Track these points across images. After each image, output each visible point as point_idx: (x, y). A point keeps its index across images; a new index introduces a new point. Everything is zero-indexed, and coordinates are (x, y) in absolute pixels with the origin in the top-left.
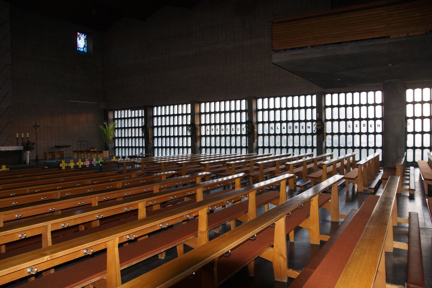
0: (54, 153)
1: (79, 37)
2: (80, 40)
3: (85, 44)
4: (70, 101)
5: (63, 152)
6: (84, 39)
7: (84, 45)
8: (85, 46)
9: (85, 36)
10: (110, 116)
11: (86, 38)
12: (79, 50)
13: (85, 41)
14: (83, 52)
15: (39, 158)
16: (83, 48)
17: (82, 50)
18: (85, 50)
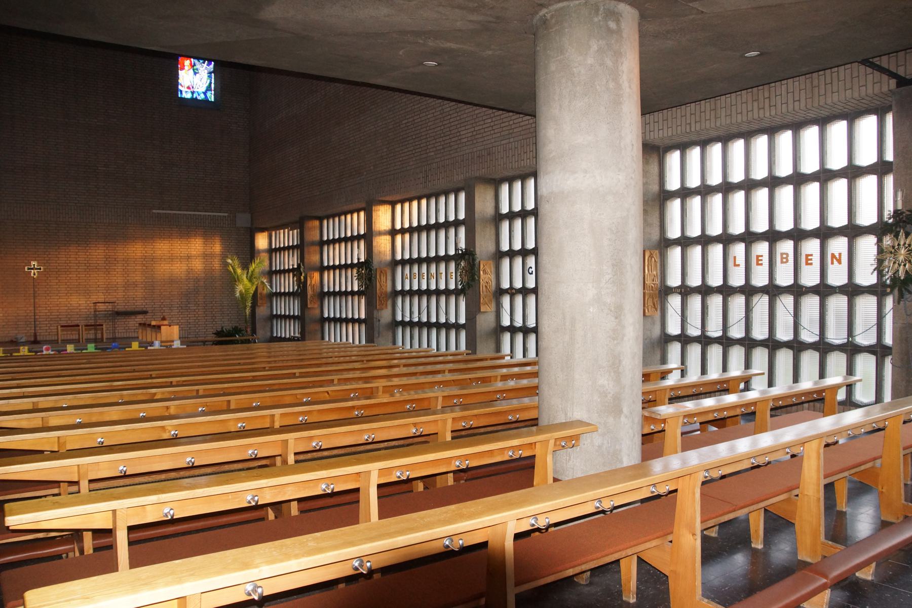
0: (102, 327)
1: (195, 67)
2: (197, 75)
3: (211, 83)
4: (154, 211)
5: (102, 325)
6: (206, 71)
7: (207, 84)
8: (209, 88)
9: (212, 66)
10: (262, 241)
11: (212, 70)
12: (194, 97)
13: (210, 77)
14: (206, 101)
16: (205, 93)
17: (202, 97)
18: (211, 97)
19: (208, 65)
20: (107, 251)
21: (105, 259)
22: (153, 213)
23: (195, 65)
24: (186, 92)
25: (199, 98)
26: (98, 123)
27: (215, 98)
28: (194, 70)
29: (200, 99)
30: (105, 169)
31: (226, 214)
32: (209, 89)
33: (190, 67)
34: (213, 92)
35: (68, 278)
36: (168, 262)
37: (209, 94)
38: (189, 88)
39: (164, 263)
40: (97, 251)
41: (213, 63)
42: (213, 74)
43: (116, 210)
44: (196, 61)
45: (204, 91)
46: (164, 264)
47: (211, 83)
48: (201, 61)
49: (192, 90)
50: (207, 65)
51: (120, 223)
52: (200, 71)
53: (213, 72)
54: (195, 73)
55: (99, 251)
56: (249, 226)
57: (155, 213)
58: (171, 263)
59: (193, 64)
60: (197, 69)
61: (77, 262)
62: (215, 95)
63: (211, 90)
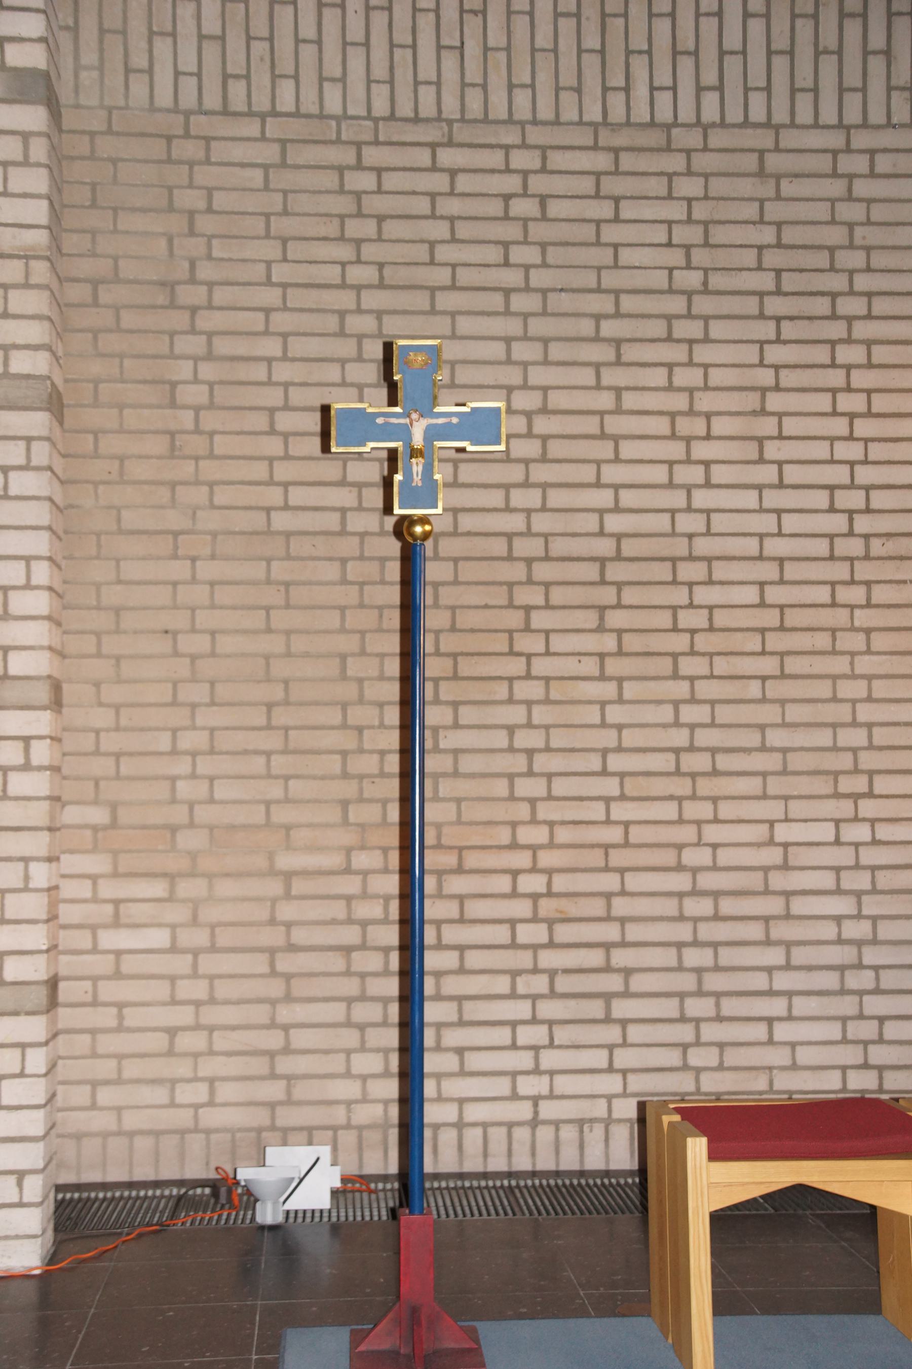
35: (689, 619)
61: (768, 474)
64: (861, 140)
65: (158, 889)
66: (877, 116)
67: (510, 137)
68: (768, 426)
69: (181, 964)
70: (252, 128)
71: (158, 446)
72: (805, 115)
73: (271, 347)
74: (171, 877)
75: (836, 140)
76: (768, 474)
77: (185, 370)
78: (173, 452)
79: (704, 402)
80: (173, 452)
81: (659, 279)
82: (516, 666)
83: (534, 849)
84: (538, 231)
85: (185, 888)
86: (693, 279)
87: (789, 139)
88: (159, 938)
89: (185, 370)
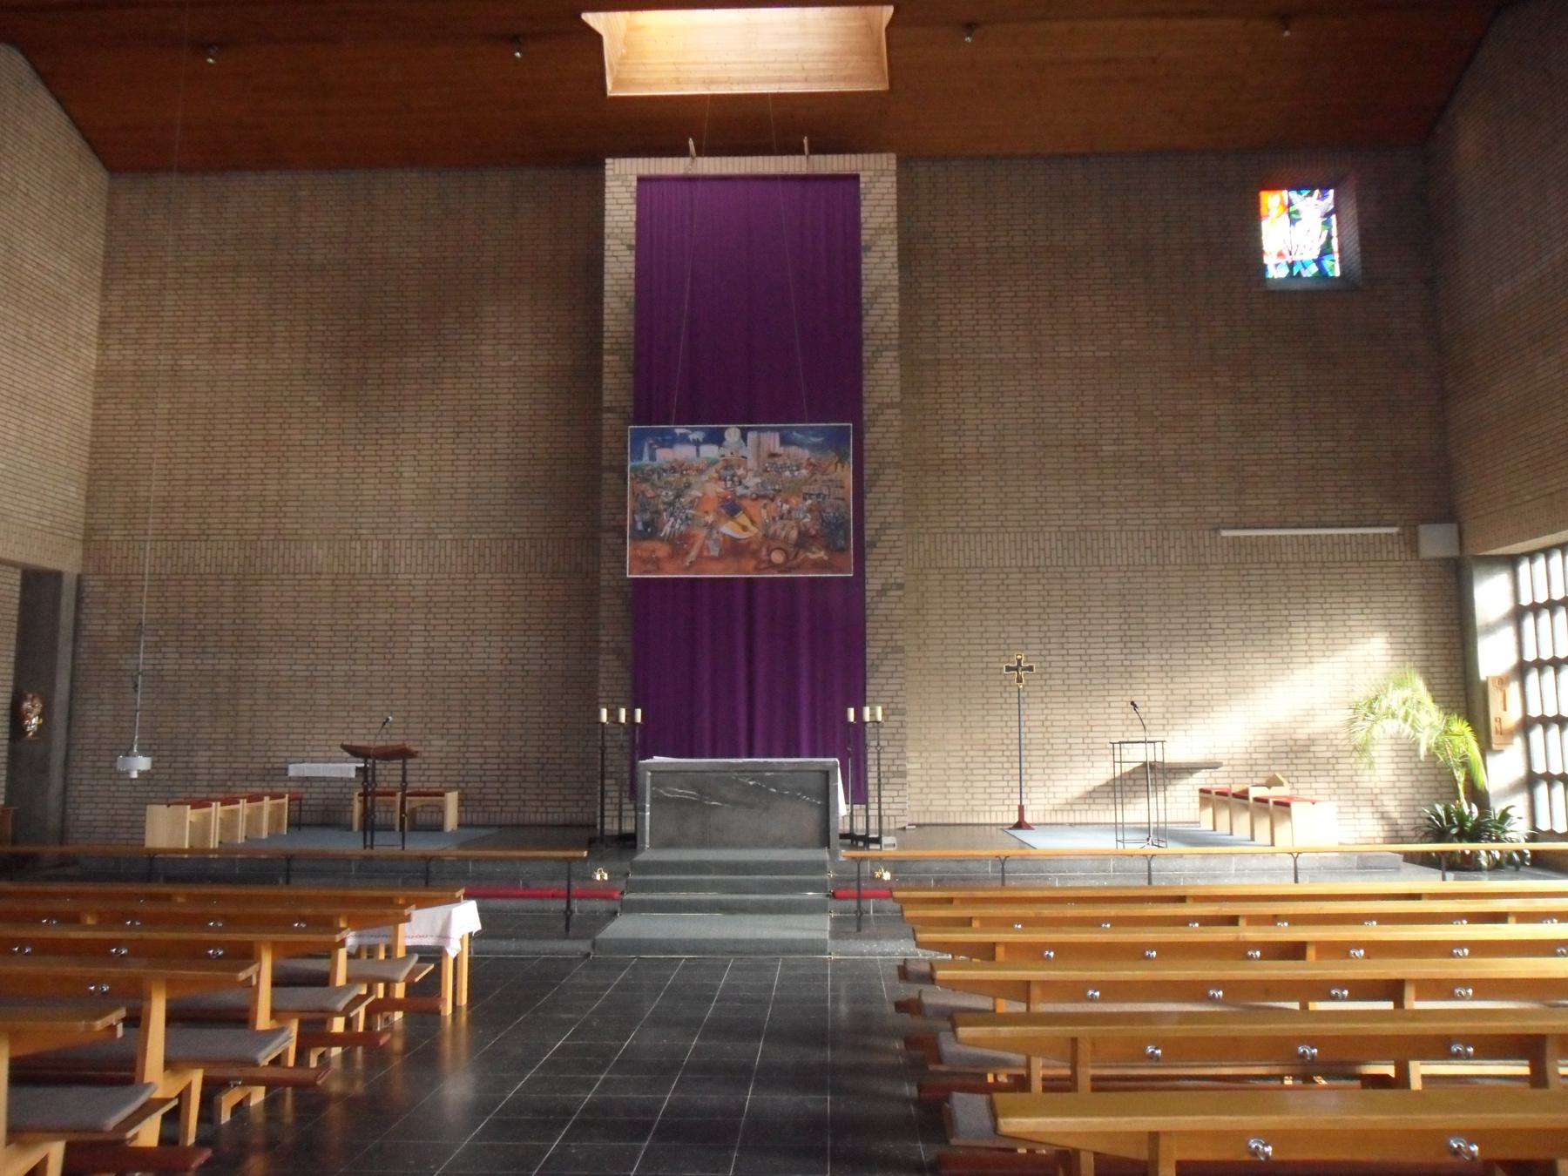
1: (1292, 209)
2: (1298, 224)
3: (1329, 237)
4: (1225, 533)
8: (1326, 250)
13: (1327, 223)
15: (1028, 819)
16: (1318, 262)
19: (1323, 197)
20: (1126, 627)
21: (1122, 645)
22: (1222, 537)
23: (1290, 204)
24: (1277, 265)
25: (1306, 274)
26: (1098, 354)
27: (1342, 268)
28: (1290, 214)
29: (1310, 275)
30: (1115, 448)
31: (1394, 530)
32: (1328, 250)
33: (1281, 209)
34: (1336, 256)
36: (1261, 648)
37: (1327, 263)
38: (1280, 255)
39: (1252, 649)
40: (1106, 627)
41: (1331, 192)
42: (1334, 218)
43: (1141, 534)
44: (1294, 194)
45: (1316, 257)
46: (1252, 652)
47: (1329, 237)
48: (1306, 193)
49: (1289, 259)
50: (1318, 199)
51: (1152, 565)
52: (1302, 216)
53: (1335, 211)
54: (1293, 222)
55: (1109, 628)
56: (1453, 552)
57: (1227, 537)
58: (1267, 649)
59: (1287, 203)
60: (1297, 212)
62: (1341, 261)
63: (1331, 252)
64: (1086, 569)
65: (917, 754)
66: (1090, 563)
67: (999, 570)
68: (1064, 640)
69: (923, 772)
70: (936, 571)
71: (915, 648)
72: (1072, 564)
73: (942, 623)
74: (921, 752)
75: (1079, 569)
76: (1064, 652)
77: (920, 630)
78: (919, 649)
79: (1049, 634)
80: (919, 649)
81: (1036, 604)
82: (1003, 701)
83: (1007, 745)
84: (1006, 593)
85: (924, 754)
86: (1045, 604)
87: (1068, 569)
88: (918, 766)
89: (920, 630)
